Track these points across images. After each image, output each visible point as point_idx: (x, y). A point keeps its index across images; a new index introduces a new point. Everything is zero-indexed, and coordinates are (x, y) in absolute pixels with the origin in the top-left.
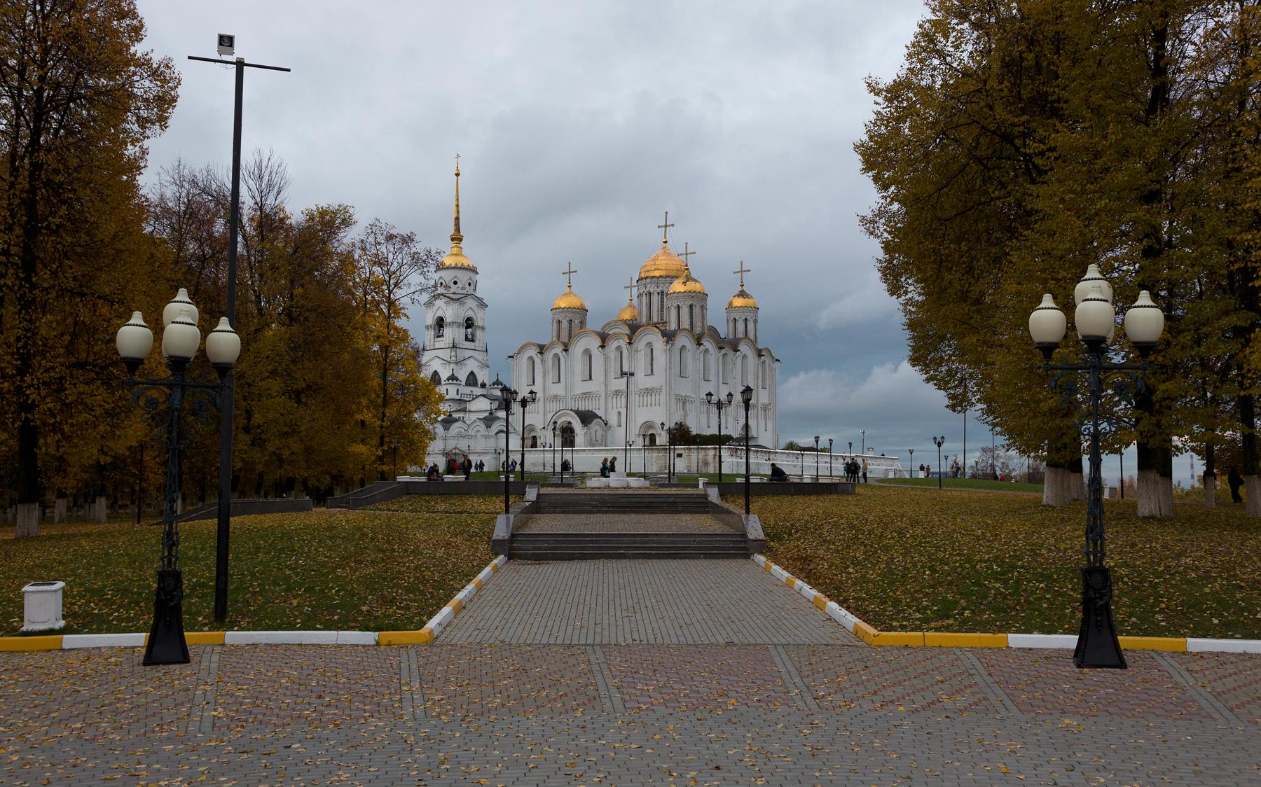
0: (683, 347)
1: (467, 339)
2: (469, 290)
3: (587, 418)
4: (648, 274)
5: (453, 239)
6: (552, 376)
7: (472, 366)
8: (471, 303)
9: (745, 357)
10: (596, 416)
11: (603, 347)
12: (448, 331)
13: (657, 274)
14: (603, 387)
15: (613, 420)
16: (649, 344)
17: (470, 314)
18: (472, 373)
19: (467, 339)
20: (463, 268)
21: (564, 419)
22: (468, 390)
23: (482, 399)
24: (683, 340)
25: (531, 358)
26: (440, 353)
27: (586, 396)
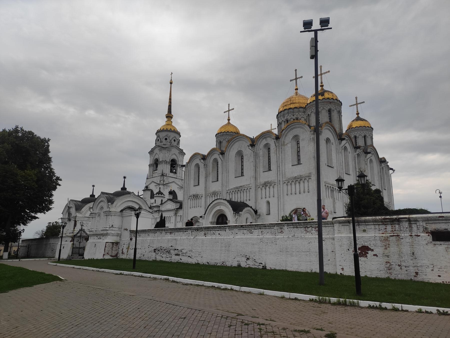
0: (328, 140)
1: (171, 171)
2: (175, 144)
3: (237, 207)
4: (285, 108)
5: (167, 117)
7: (174, 187)
8: (174, 151)
9: (371, 161)
10: (247, 206)
11: (253, 145)
12: (159, 166)
13: (292, 106)
14: (253, 181)
15: (262, 209)
17: (174, 157)
19: (171, 171)
20: (170, 131)
21: (218, 208)
23: (169, 202)
25: (197, 166)
26: (155, 180)
27: (239, 189)
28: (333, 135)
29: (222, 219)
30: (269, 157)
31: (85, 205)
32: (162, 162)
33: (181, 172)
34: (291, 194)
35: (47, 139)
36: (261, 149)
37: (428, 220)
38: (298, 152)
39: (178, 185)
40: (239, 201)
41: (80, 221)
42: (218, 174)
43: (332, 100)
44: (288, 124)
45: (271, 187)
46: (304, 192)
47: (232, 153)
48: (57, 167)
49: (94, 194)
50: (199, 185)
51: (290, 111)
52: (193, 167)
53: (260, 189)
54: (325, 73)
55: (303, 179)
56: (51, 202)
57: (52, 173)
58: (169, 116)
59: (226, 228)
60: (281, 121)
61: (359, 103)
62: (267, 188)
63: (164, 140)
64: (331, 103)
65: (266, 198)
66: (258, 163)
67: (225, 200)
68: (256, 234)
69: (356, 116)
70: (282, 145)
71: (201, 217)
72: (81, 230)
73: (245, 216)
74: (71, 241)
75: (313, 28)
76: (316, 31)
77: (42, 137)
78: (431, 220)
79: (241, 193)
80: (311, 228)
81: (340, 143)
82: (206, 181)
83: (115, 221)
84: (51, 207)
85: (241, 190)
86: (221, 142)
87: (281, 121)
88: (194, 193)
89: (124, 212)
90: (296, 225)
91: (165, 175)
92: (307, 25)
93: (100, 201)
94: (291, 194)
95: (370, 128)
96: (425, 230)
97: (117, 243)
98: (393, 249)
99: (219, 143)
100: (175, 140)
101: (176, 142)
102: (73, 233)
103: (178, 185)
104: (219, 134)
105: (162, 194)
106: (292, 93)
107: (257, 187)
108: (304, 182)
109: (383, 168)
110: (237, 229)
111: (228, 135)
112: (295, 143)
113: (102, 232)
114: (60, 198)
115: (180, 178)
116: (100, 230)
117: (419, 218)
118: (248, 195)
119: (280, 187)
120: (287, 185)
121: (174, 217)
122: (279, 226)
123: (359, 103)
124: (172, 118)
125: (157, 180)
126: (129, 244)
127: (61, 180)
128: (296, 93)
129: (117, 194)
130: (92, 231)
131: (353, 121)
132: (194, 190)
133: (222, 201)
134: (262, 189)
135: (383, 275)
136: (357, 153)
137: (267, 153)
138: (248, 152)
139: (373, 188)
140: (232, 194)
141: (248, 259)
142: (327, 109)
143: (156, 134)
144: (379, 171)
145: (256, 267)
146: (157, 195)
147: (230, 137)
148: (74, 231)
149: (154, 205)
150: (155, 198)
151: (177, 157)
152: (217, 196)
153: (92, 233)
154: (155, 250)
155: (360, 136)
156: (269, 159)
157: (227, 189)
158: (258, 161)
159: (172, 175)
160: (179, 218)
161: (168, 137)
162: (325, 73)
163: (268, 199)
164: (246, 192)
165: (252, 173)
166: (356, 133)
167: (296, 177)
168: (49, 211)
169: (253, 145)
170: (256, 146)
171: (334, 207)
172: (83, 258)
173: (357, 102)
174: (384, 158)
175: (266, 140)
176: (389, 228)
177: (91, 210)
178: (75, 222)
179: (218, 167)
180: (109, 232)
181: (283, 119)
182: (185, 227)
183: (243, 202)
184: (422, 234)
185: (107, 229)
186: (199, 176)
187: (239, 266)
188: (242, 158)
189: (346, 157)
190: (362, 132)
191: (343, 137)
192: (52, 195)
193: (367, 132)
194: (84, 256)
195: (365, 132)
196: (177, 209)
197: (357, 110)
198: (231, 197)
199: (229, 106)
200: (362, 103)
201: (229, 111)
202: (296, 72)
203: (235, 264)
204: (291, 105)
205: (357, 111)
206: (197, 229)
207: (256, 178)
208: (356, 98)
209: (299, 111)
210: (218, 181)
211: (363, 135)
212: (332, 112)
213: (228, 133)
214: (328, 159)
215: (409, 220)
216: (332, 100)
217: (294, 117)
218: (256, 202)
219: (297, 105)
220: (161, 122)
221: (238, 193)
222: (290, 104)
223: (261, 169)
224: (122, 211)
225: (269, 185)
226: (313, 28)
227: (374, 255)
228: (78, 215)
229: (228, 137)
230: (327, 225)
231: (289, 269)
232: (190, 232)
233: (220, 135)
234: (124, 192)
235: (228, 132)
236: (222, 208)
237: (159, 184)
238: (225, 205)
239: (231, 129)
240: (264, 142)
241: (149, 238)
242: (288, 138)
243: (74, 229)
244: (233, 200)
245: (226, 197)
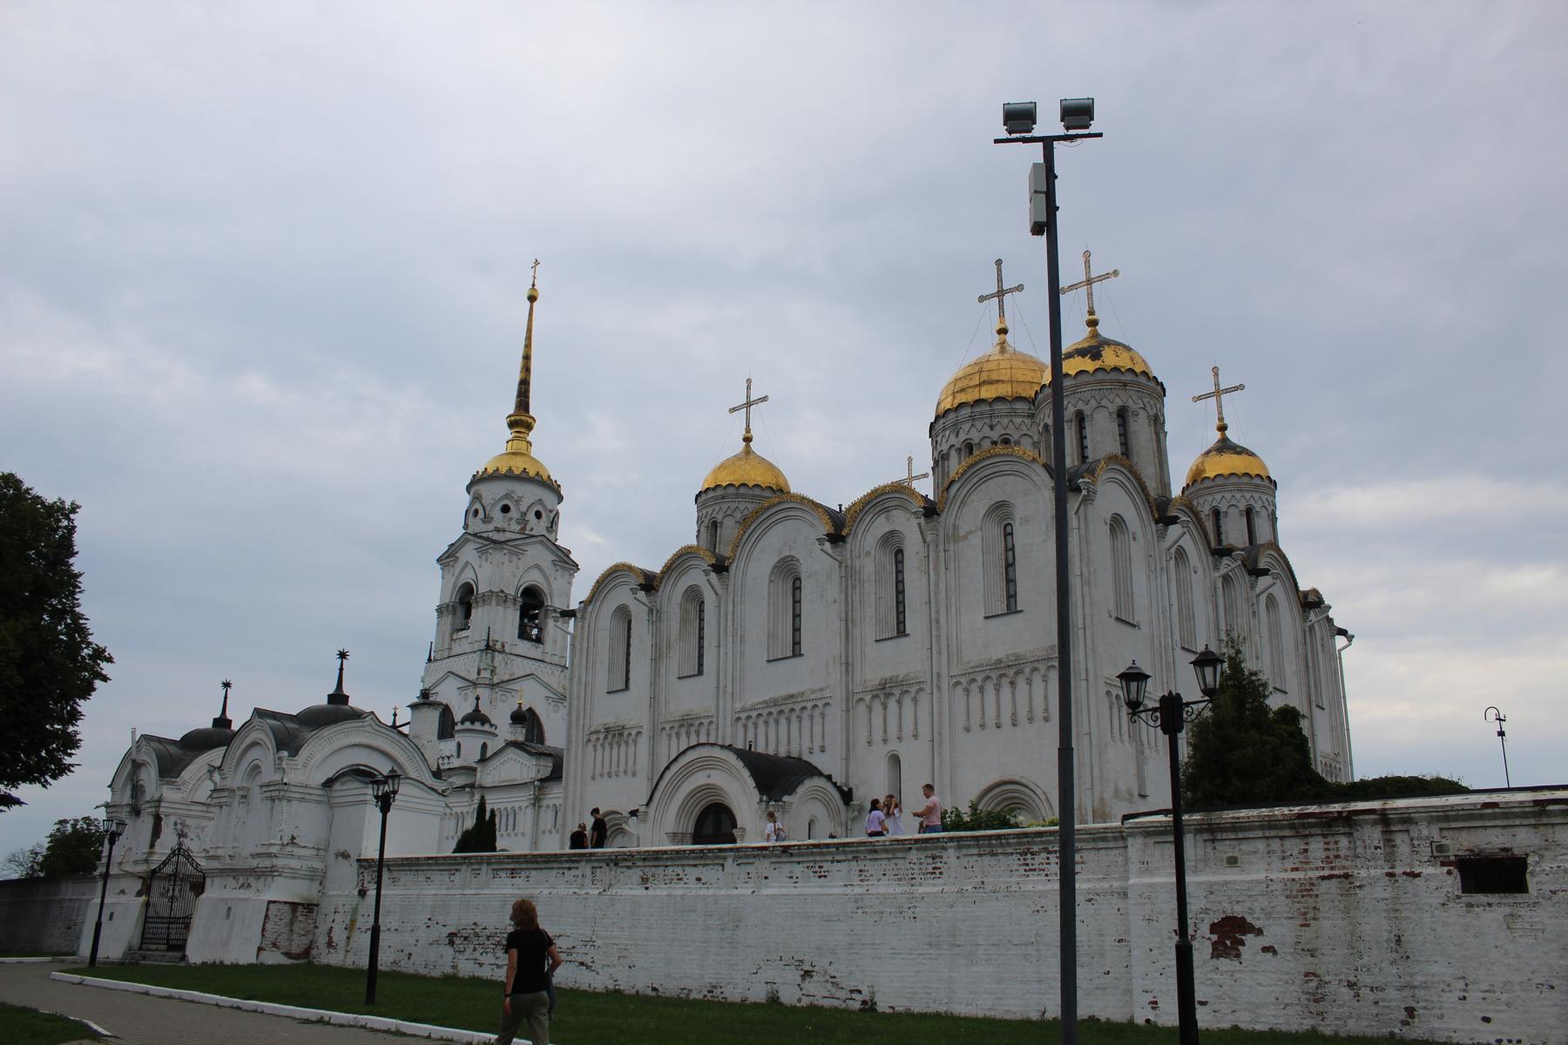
0: (1117, 523)
1: (523, 634)
2: (539, 527)
5: (512, 425)
6: (679, 657)
7: (531, 696)
8: (536, 554)
9: (1271, 601)
10: (814, 772)
11: (836, 538)
13: (988, 393)
14: (836, 675)
15: (873, 786)
16: (1001, 511)
17: (534, 578)
19: (523, 634)
20: (524, 478)
21: (699, 779)
23: (513, 753)
24: (1112, 497)
25: (623, 614)
26: (458, 665)
27: (782, 708)
28: (1135, 504)
29: (714, 823)
30: (900, 582)
31: (195, 757)
32: (487, 598)
33: (559, 635)
34: (983, 726)
35: (67, 505)
36: (868, 553)
37: (1447, 819)
38: (1010, 565)
39: (547, 686)
40: (782, 753)
41: (173, 819)
42: (701, 648)
43: (1129, 377)
44: (970, 460)
45: (907, 701)
46: (1031, 720)
47: (756, 567)
48: (100, 610)
49: (229, 716)
50: (627, 687)
51: (978, 409)
52: (605, 614)
53: (862, 708)
54: (1101, 278)
55: (1027, 670)
56: (71, 742)
57: (78, 629)
58: (521, 422)
59: (725, 858)
60: (945, 447)
61: (1227, 391)
62: (892, 703)
63: (497, 514)
64: (1125, 385)
65: (885, 741)
66: (857, 605)
67: (730, 748)
68: (839, 883)
69: (1218, 435)
70: (947, 540)
71: (634, 813)
72: (178, 851)
73: (806, 812)
74: (139, 894)
75: (1038, 131)
76: (1048, 142)
77: (50, 498)
78: (1457, 818)
79: (789, 720)
80: (1044, 855)
81: (1162, 535)
82: (656, 673)
83: (303, 820)
84: (67, 760)
85: (792, 710)
86: (714, 525)
87: (945, 447)
88: (610, 721)
89: (337, 786)
90: (990, 845)
91: (498, 646)
92: (1019, 120)
93: (248, 741)
94: (983, 726)
95: (1266, 483)
96: (1439, 854)
97: (310, 907)
98: (1330, 925)
99: (710, 527)
100: (538, 515)
101: (544, 522)
102: (146, 861)
103: (547, 686)
104: (711, 494)
105: (484, 720)
106: (986, 346)
107: (851, 700)
108: (1029, 682)
109: (1311, 628)
110: (767, 863)
111: (743, 496)
112: (997, 532)
113: (254, 863)
114: (106, 728)
115: (556, 660)
116: (245, 853)
117: (1417, 810)
118: (817, 729)
119: (940, 702)
120: (967, 691)
121: (530, 811)
122: (925, 849)
123: (1227, 391)
124: (529, 427)
125: (468, 666)
126: (355, 911)
127: (110, 660)
128: (1003, 344)
129: (314, 720)
130: (216, 858)
131: (1207, 453)
132: (608, 711)
133: (716, 752)
134: (870, 709)
135: (1293, 1021)
136: (1223, 571)
137: (891, 567)
138: (817, 563)
139: (1274, 702)
140: (756, 725)
141: (807, 974)
142: (1113, 408)
143: (468, 489)
144: (1300, 637)
145: (836, 1003)
146: (468, 725)
147: (751, 507)
148: (151, 853)
149: (456, 763)
150: (458, 738)
151: (547, 578)
152: (698, 733)
153: (215, 864)
154: (452, 935)
155: (1232, 511)
156: (900, 592)
157: (738, 706)
158: (856, 598)
159: (525, 647)
160: (551, 815)
161: (512, 504)
162: (1101, 278)
163: (894, 745)
164: (812, 717)
165: (836, 647)
166: (1218, 497)
167: (999, 661)
168: (63, 779)
169: (836, 538)
170: (849, 540)
171: (1140, 776)
172: (184, 957)
173: (1217, 384)
174: (1315, 592)
175: (887, 519)
176: (1317, 847)
177: (217, 777)
178: (158, 820)
179: (701, 620)
180: (279, 862)
181: (953, 440)
182: (568, 850)
183: (799, 759)
184: (1428, 870)
185: (274, 850)
186: (628, 654)
187: (774, 1000)
188: (797, 589)
189: (1183, 588)
190: (1238, 495)
191: (1172, 513)
192: (74, 716)
193: (1256, 496)
194: (188, 953)
195: (1248, 495)
196: (541, 780)
197: (1220, 413)
198: (751, 737)
199: (749, 388)
200: (1236, 389)
201: (749, 404)
202: (999, 271)
203: (758, 994)
204: (983, 389)
205: (1221, 419)
206: (615, 861)
207: (848, 665)
208: (1216, 371)
209: (1013, 413)
210: (700, 672)
211: (1242, 507)
213: (743, 490)
214: (1117, 592)
215: (1384, 818)
216: (1129, 377)
218: (847, 759)
219: (1004, 390)
220: (489, 443)
221: (777, 722)
222: (980, 385)
223: (867, 631)
224: (329, 784)
225: (897, 692)
226: (1038, 131)
227: (1266, 949)
228: (168, 793)
229: (743, 505)
230: (1101, 845)
231: (961, 1009)
232: (585, 868)
233: (715, 498)
234: (338, 710)
235: (744, 485)
236: (717, 778)
237: (474, 684)
238: (729, 770)
239: (756, 476)
240: (881, 526)
241: (433, 889)
242: (971, 514)
243: (152, 846)
244: (761, 749)
245: (734, 736)
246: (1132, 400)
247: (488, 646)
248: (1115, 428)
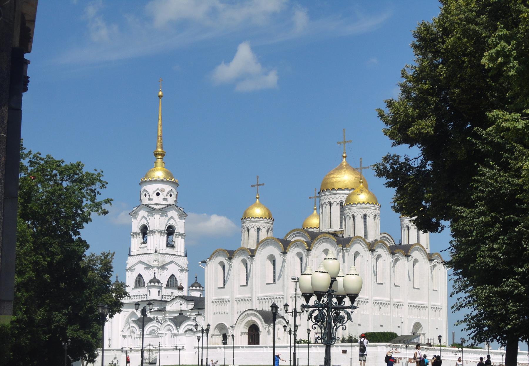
2: (171, 201)
12: (150, 238)
17: (171, 222)
18: (172, 276)
21: (249, 318)
22: (168, 292)
26: (144, 259)
32: (153, 232)
39: (179, 266)
71: (232, 327)
100: (171, 195)
103: (179, 266)
105: (158, 282)
142: (362, 215)
146: (152, 284)
159: (170, 250)
170: (288, 253)
199: (258, 179)
212: (367, 217)
217: (338, 201)
224: (186, 331)
244: (264, 309)
246: (368, 212)
247: (156, 251)
248: (362, 220)
